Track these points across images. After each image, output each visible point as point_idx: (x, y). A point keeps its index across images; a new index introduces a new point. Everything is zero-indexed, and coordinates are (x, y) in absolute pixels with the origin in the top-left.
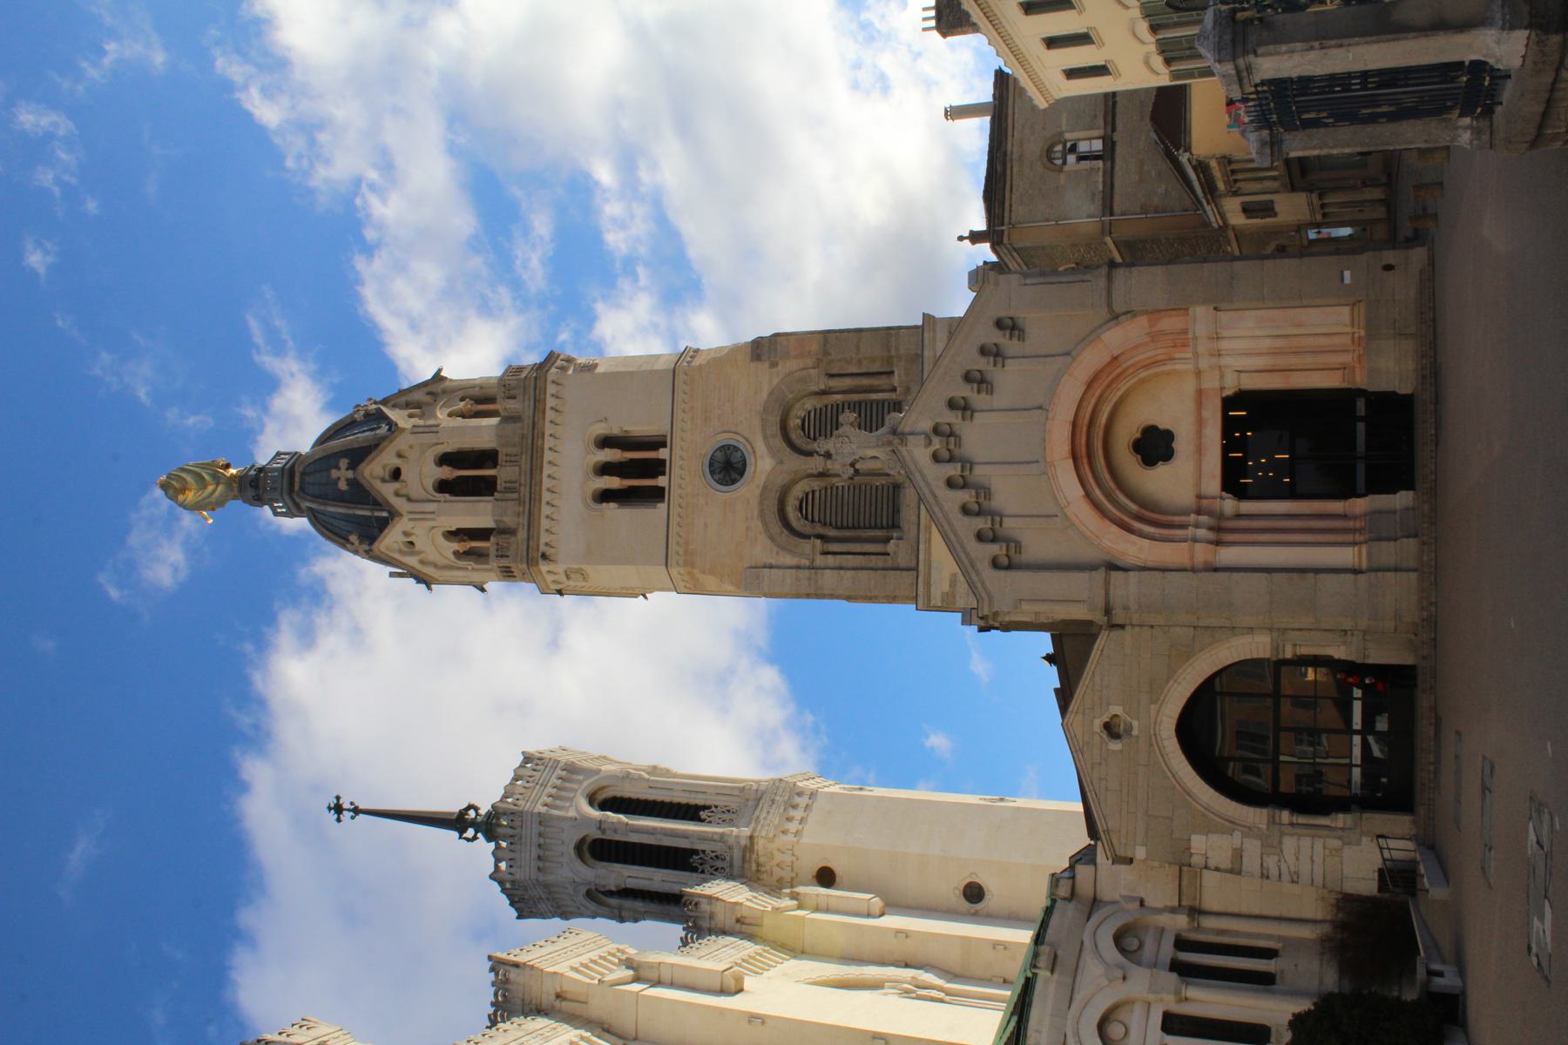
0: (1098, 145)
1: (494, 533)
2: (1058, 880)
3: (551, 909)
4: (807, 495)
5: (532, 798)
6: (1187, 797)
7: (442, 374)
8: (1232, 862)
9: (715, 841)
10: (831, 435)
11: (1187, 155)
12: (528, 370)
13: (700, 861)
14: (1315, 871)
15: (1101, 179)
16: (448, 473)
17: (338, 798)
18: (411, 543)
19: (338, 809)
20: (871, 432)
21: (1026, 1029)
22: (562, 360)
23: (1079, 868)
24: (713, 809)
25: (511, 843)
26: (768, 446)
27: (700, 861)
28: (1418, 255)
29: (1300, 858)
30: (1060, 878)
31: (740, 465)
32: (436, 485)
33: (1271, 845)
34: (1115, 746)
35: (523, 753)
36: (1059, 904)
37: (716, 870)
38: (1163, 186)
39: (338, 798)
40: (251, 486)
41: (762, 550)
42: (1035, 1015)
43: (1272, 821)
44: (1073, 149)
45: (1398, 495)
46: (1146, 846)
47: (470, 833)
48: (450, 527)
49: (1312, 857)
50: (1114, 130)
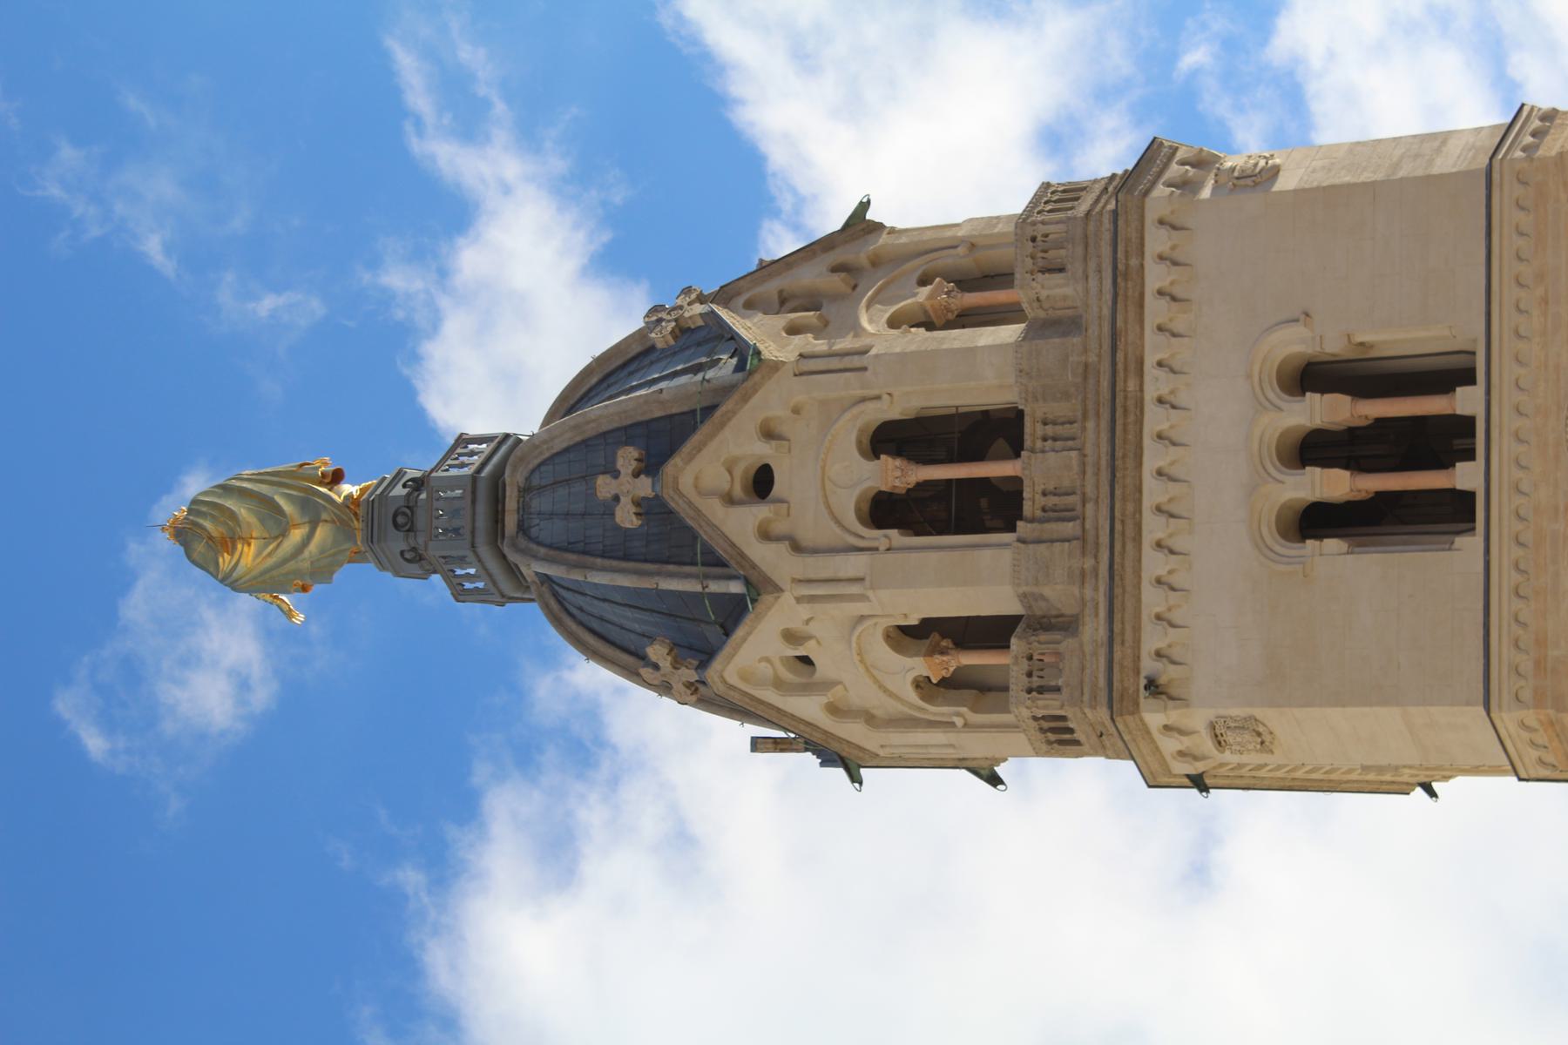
7: (869, 216)
16: (896, 474)
18: (806, 660)
22: (1183, 163)
32: (866, 507)
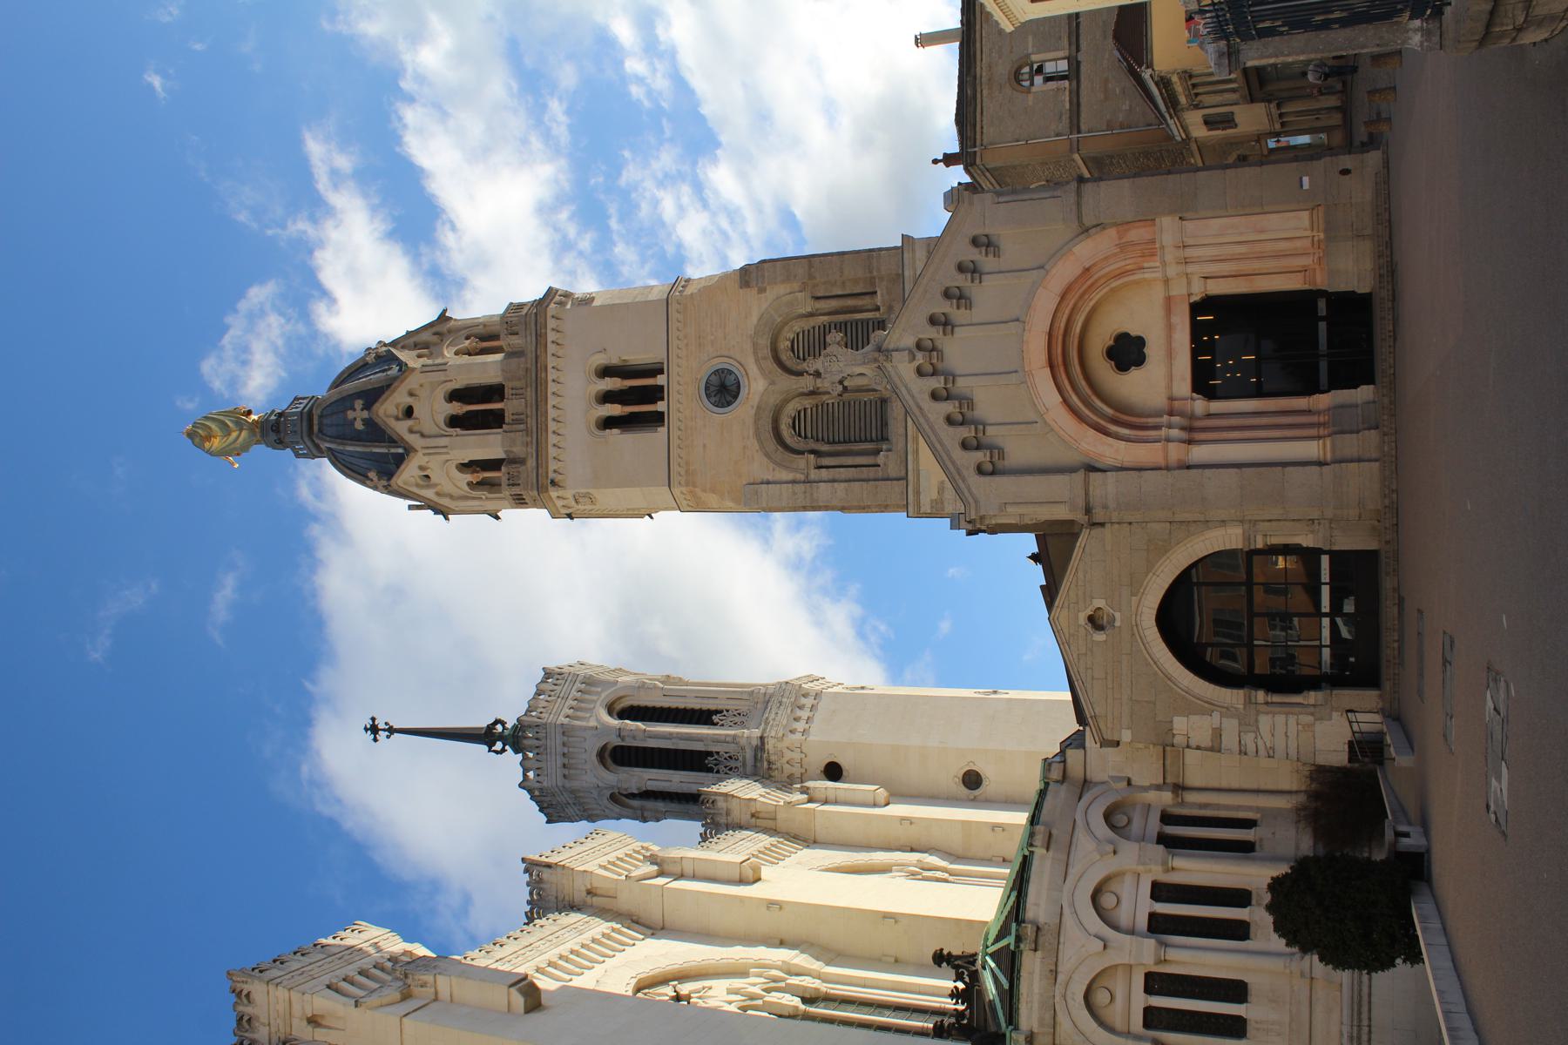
0: (1063, 66)
1: (504, 464)
2: (1050, 764)
3: (578, 812)
4: (799, 412)
5: (554, 710)
6: (1169, 682)
7: (447, 315)
8: (1212, 741)
9: (728, 742)
10: (820, 355)
11: (1149, 71)
12: (528, 307)
14: (1289, 745)
15: (1067, 99)
16: (458, 408)
17: (373, 719)
18: (427, 477)
19: (374, 729)
20: (857, 350)
21: (1025, 902)
22: (560, 296)
23: (1069, 752)
24: (725, 713)
25: (538, 754)
26: (761, 369)
28: (1374, 158)
29: (1275, 734)
30: (1053, 762)
31: (734, 388)
32: (448, 421)
33: (1247, 723)
34: (1100, 637)
35: (543, 669)
36: (1052, 787)
37: (731, 769)
38: (1127, 102)
39: (373, 719)
40: (273, 431)
41: (760, 467)
42: (1032, 889)
43: (1248, 702)
44: (1040, 70)
45: (1359, 389)
46: (1131, 728)
47: (499, 746)
48: (463, 460)
49: (1286, 733)
50: (1078, 50)
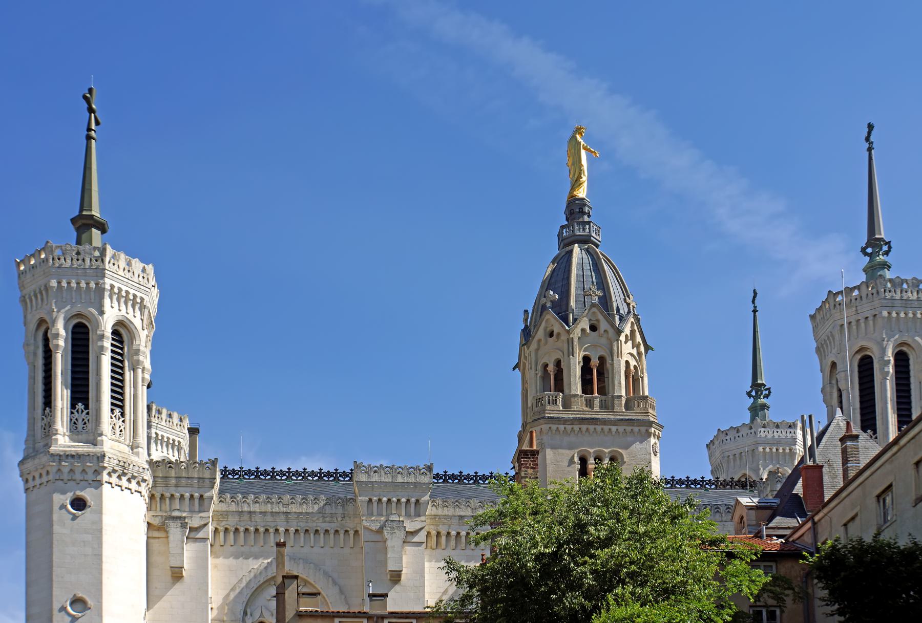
13: (80, 411)
27: (80, 411)
